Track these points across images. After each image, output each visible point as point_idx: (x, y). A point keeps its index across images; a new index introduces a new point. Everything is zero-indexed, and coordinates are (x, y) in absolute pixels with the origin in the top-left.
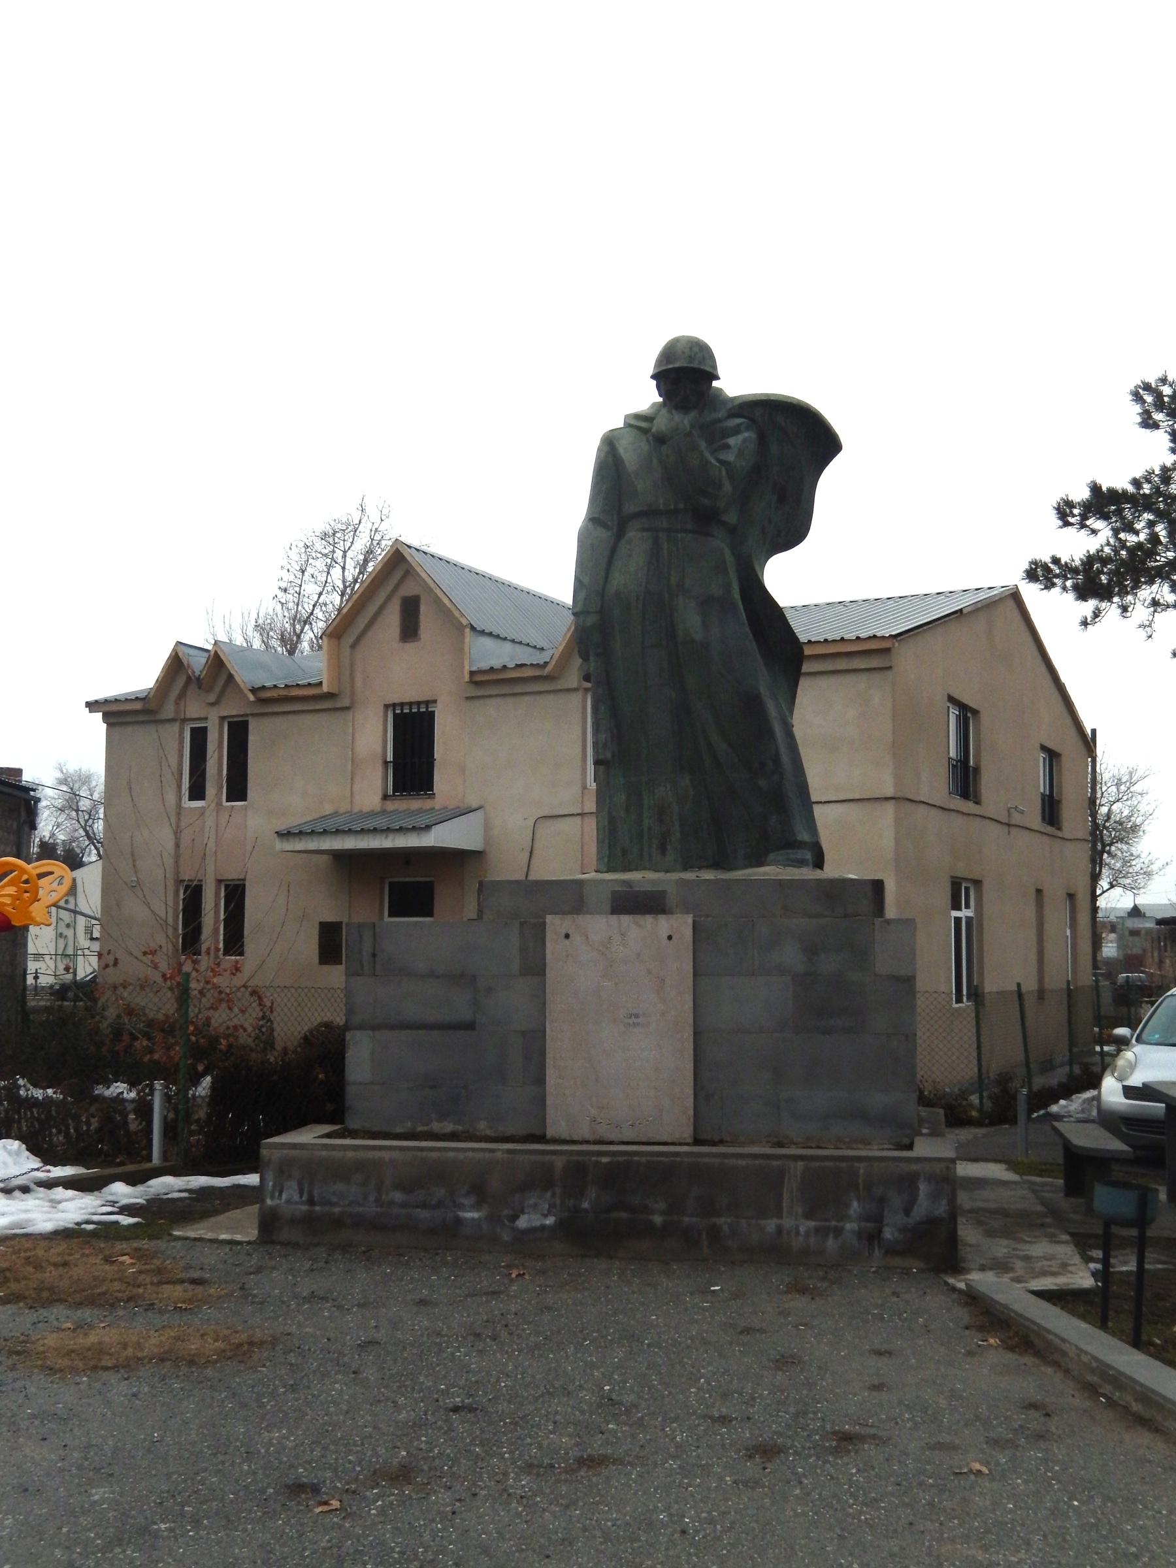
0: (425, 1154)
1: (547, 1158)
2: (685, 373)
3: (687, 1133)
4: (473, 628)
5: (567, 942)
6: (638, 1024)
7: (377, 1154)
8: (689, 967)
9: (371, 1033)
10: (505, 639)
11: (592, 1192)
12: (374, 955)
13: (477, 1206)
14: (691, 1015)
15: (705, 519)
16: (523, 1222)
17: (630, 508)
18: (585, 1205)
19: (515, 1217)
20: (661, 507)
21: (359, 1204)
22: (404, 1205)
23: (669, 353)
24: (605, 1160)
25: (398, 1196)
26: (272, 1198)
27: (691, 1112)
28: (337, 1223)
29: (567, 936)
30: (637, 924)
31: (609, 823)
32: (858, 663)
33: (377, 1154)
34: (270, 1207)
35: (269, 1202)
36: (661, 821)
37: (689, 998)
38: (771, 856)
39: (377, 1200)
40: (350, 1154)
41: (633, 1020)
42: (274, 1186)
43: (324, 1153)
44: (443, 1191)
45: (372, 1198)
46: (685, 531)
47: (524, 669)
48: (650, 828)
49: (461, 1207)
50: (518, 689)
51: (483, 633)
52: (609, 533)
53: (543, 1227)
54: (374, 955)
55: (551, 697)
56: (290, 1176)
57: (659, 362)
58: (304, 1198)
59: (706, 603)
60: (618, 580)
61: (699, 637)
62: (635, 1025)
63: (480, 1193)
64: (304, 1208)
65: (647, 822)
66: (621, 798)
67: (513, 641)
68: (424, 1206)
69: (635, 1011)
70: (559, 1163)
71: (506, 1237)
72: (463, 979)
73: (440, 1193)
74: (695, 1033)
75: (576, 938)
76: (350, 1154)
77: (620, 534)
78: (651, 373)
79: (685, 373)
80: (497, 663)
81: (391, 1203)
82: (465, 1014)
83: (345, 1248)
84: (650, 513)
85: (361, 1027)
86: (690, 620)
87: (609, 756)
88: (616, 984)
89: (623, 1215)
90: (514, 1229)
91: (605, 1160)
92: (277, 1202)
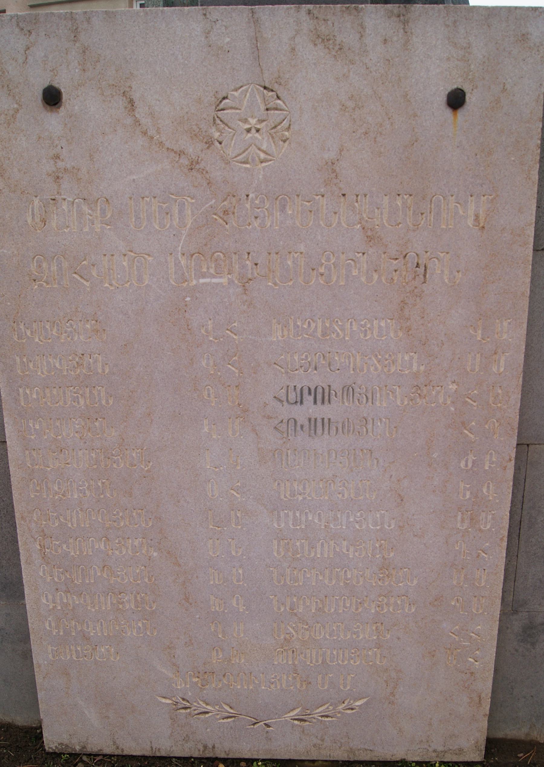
5: (53, 121)
6: (326, 424)
14: (516, 397)
27: (486, 686)
29: (52, 98)
30: (322, 39)
41: (310, 409)
62: (315, 425)
69: (316, 380)
74: (522, 446)
88: (245, 282)
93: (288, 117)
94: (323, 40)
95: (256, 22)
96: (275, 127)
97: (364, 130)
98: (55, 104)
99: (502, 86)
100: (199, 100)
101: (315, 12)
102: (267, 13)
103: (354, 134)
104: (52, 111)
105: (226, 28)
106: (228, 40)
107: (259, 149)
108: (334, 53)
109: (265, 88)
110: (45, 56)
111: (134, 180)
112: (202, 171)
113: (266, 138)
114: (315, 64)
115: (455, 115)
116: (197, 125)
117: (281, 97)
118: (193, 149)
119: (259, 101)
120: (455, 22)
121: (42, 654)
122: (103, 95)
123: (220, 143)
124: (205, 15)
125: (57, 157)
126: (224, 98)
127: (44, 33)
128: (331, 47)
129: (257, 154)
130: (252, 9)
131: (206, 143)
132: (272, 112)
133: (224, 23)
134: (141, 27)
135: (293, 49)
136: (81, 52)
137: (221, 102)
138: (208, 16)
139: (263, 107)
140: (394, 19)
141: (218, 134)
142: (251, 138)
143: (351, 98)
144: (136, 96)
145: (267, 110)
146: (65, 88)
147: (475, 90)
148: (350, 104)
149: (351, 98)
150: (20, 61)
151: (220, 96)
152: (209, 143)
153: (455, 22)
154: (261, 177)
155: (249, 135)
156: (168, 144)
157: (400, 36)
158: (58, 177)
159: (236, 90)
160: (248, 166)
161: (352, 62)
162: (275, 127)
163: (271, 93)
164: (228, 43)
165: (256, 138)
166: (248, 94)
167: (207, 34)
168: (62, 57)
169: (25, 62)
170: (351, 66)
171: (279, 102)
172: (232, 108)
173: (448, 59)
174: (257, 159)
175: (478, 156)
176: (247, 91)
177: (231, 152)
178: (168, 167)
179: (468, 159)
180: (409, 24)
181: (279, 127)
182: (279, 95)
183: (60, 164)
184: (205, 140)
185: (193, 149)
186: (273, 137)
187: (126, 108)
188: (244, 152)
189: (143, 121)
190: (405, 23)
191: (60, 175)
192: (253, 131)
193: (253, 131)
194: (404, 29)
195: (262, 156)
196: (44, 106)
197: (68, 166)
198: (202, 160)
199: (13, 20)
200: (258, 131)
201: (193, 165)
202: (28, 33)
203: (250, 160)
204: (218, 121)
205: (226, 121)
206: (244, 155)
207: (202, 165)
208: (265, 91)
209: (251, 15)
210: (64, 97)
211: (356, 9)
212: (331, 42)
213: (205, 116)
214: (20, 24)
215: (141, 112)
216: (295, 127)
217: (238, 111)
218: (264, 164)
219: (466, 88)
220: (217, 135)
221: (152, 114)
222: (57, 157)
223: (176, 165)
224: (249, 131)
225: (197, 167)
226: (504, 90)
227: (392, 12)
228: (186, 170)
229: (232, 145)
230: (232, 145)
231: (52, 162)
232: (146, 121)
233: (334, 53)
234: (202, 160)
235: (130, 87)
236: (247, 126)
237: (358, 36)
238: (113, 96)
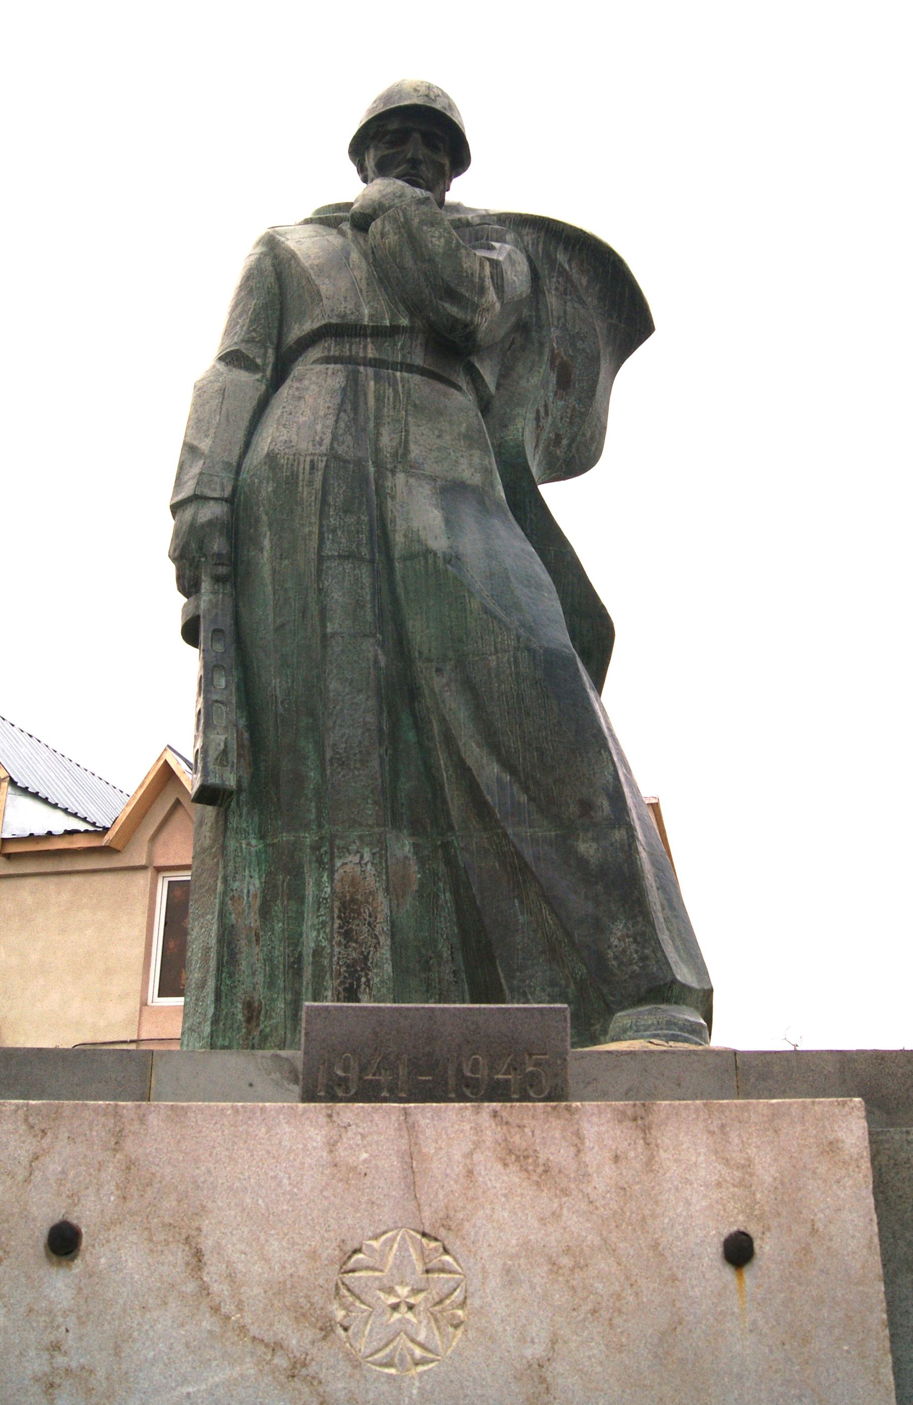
4: (13, 783)
5: (60, 1284)
10: (55, 806)
15: (450, 347)
17: (297, 331)
20: (366, 321)
29: (64, 1242)
30: (516, 1156)
31: (220, 940)
36: (348, 935)
38: (622, 1018)
46: (410, 368)
47: (76, 837)
48: (317, 952)
50: (65, 865)
51: (25, 791)
52: (258, 376)
55: (109, 878)
59: (451, 492)
60: (270, 437)
61: (439, 543)
65: (310, 939)
66: (251, 884)
67: (65, 810)
77: (279, 376)
80: (40, 831)
84: (341, 331)
86: (421, 516)
87: (231, 781)
93: (463, 1284)
94: (518, 1157)
95: (410, 1128)
96: (441, 1302)
97: (590, 1306)
98: (67, 1254)
99: (809, 1225)
100: (314, 1255)
101: (504, 1114)
102: (429, 1115)
103: (575, 1313)
104: (59, 1264)
105: (363, 1137)
106: (365, 1156)
107: (413, 1341)
108: (535, 1178)
109: (424, 1235)
110: (63, 1172)
111: (188, 1394)
112: (313, 1380)
113: (425, 1322)
114: (505, 1196)
115: (740, 1276)
116: (307, 1297)
117: (451, 1251)
118: (297, 1339)
119: (414, 1257)
120: (723, 1126)
122: (151, 1240)
123: (346, 1329)
124: (330, 1116)
125: (56, 1347)
126: (356, 1251)
127: (67, 1135)
128: (530, 1168)
129: (409, 1349)
130: (405, 1109)
131: (321, 1329)
132: (436, 1275)
133: (360, 1130)
134: (227, 1132)
135: (470, 1173)
136: (124, 1167)
137: (350, 1257)
138: (335, 1118)
139: (419, 1267)
140: (630, 1124)
141: (343, 1313)
142: (400, 1320)
143: (568, 1250)
144: (207, 1244)
145: (427, 1271)
146: (88, 1226)
147: (768, 1234)
148: (566, 1261)
149: (568, 1250)
150: (20, 1178)
151: (349, 1248)
152: (327, 1329)
153: (723, 1126)
154: (415, 1391)
155: (397, 1316)
156: (254, 1331)
157: (640, 1150)
158: (52, 1385)
159: (376, 1237)
160: (392, 1371)
161: (565, 1192)
162: (441, 1302)
163: (433, 1244)
164: (365, 1161)
165: (409, 1321)
166: (396, 1246)
167: (332, 1146)
168: (90, 1175)
169: (27, 1180)
170: (564, 1199)
171: (447, 1258)
172: (368, 1268)
173: (719, 1185)
174: (408, 1358)
175: (787, 1347)
176: (393, 1239)
177: (363, 1346)
178: (252, 1372)
179: (771, 1351)
180: (654, 1132)
181: (448, 1302)
182: (448, 1247)
183: (60, 1360)
184: (319, 1324)
185: (297, 1339)
186: (436, 1320)
187: (188, 1264)
188: (387, 1345)
189: (215, 1288)
190: (646, 1130)
191: (57, 1381)
192: (404, 1308)
193: (404, 1308)
194: (644, 1139)
195: (418, 1352)
196: (47, 1255)
197: (74, 1364)
198: (312, 1360)
199: (20, 1112)
200: (411, 1307)
201: (297, 1369)
202: (40, 1134)
203: (396, 1360)
204: (344, 1291)
205: (357, 1291)
206: (387, 1351)
207: (313, 1368)
208: (424, 1241)
209: (402, 1118)
210: (85, 1241)
211: (568, 1108)
212: (530, 1160)
213: (321, 1281)
214: (31, 1118)
215: (213, 1271)
216: (475, 1302)
217: (377, 1274)
218: (421, 1369)
219: (753, 1230)
220: (340, 1314)
221: (231, 1277)
222: (56, 1347)
223: (267, 1367)
224: (395, 1307)
225: (304, 1372)
226: (814, 1231)
227: (624, 1113)
228: (282, 1378)
229: (367, 1332)
230: (367, 1332)
231: (46, 1356)
232: (221, 1289)
233: (535, 1178)
234: (312, 1360)
235: (199, 1229)
236: (393, 1300)
237: (573, 1150)
238: (167, 1243)
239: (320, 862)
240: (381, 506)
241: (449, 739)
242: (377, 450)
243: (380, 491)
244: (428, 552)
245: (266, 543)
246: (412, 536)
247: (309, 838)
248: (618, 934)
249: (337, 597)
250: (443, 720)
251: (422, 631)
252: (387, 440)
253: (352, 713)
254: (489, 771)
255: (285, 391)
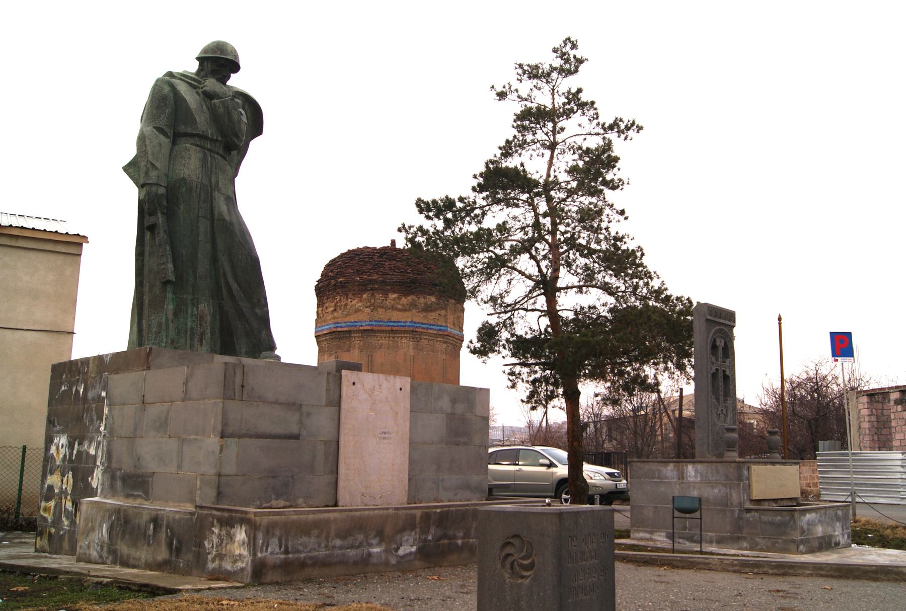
0: (353, 513)
1: (413, 511)
2: (219, 62)
3: (405, 500)
5: (354, 387)
7: (326, 515)
8: (408, 406)
9: (237, 440)
11: (432, 530)
12: (243, 386)
13: (379, 544)
16: (401, 552)
17: (182, 128)
18: (430, 538)
19: (397, 549)
21: (315, 549)
22: (341, 548)
23: (220, 47)
24: (438, 510)
25: (338, 542)
26: (261, 552)
28: (303, 565)
29: (354, 384)
32: (59, 248)
33: (326, 515)
34: (260, 558)
35: (259, 555)
37: (408, 424)
39: (326, 546)
40: (311, 517)
42: (263, 544)
43: (295, 517)
44: (362, 536)
45: (323, 545)
46: (218, 154)
48: (192, 328)
49: (371, 545)
52: (168, 140)
53: (411, 553)
54: (243, 386)
56: (273, 535)
57: (205, 51)
58: (282, 549)
62: (384, 438)
63: (381, 535)
64: (283, 556)
65: (189, 324)
68: (351, 547)
70: (418, 513)
71: (393, 561)
72: (295, 406)
73: (361, 537)
75: (358, 385)
76: (311, 517)
78: (197, 55)
79: (219, 62)
81: (334, 547)
82: (294, 429)
83: (309, 580)
85: (231, 436)
89: (446, 541)
90: (397, 556)
91: (438, 510)
92: (264, 554)
121: (341, 484)
239: (193, 304)
240: (212, 201)
241: (225, 275)
242: (211, 183)
243: (211, 196)
244: (224, 220)
245: (182, 207)
246: (220, 214)
247: (190, 297)
248: (264, 333)
249: (202, 229)
250: (224, 270)
251: (220, 245)
252: (213, 180)
253: (203, 265)
254: (235, 286)
255: (176, 148)
